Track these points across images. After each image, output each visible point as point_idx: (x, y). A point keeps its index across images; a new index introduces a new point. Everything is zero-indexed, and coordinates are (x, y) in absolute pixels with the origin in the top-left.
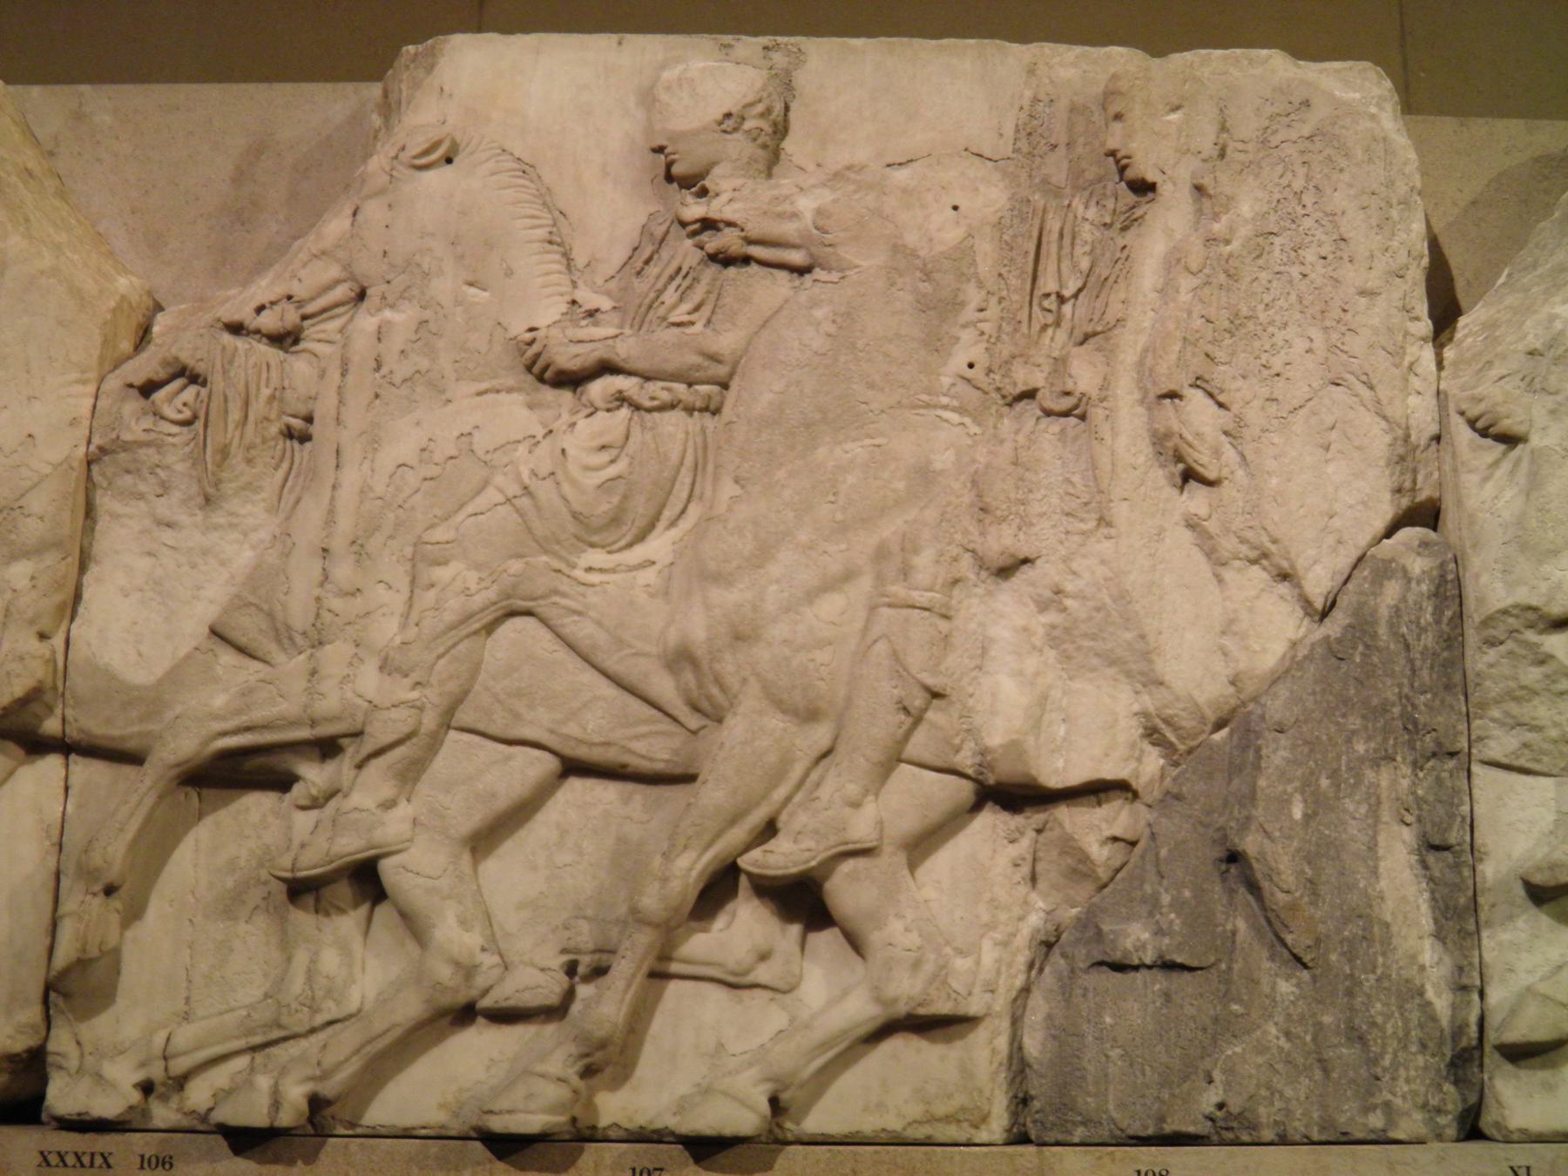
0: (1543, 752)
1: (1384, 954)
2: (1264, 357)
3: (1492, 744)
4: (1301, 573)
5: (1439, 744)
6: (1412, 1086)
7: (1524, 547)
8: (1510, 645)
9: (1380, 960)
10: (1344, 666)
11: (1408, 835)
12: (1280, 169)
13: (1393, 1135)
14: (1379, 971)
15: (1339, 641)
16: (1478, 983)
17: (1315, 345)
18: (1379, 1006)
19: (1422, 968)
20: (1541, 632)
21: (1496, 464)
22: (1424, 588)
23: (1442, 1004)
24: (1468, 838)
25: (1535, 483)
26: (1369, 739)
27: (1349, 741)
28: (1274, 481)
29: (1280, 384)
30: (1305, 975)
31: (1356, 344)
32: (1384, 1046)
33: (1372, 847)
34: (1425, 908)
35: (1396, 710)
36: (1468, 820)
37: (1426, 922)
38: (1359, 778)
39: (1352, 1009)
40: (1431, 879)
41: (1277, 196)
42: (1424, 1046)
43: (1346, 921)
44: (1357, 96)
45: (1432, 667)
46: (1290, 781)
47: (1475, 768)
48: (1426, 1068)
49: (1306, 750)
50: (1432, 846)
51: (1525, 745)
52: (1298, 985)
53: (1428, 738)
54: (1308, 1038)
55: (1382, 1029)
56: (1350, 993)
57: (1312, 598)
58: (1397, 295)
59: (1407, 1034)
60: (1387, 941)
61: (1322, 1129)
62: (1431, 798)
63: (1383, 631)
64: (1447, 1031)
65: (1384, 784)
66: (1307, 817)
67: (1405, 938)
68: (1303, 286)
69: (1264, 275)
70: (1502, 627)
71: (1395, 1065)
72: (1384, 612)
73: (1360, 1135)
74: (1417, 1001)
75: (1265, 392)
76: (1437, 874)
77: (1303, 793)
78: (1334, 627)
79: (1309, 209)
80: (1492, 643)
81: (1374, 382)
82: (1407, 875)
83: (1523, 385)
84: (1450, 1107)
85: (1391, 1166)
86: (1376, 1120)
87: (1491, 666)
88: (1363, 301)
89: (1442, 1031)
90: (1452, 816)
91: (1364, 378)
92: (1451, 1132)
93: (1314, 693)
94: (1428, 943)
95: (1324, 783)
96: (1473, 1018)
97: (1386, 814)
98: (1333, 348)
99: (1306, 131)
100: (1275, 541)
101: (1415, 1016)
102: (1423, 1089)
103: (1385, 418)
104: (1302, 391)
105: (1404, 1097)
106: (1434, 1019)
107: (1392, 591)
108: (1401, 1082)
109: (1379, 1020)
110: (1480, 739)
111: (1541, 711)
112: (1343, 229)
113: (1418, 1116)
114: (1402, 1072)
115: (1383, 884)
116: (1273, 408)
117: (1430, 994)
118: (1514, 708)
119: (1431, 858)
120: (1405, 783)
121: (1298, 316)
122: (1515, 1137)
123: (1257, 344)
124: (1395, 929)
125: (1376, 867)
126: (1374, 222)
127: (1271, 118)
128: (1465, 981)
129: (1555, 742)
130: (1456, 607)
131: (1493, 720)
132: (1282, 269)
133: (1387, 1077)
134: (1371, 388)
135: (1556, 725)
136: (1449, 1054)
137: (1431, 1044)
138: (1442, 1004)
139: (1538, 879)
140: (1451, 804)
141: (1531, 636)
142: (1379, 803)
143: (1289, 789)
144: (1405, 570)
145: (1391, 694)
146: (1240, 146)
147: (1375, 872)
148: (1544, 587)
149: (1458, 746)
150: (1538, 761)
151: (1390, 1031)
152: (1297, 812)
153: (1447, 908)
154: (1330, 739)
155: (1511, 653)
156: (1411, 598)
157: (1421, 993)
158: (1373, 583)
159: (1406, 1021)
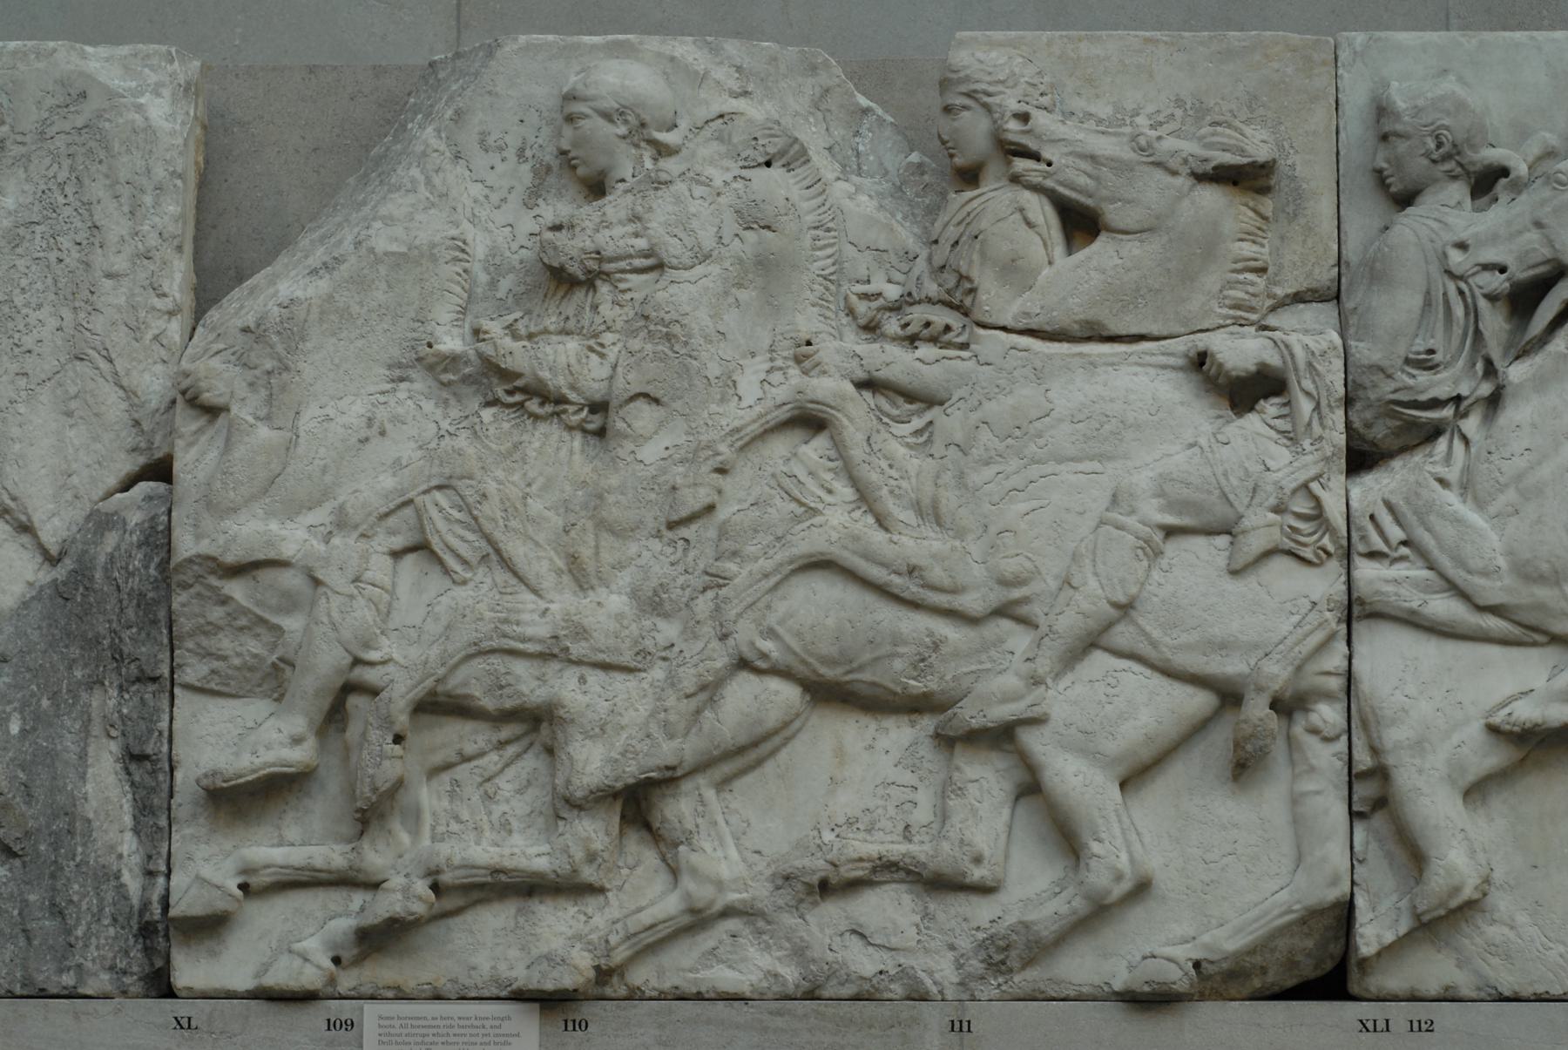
0: (228, 677)
1: (84, 845)
2: (17, 336)
3: (188, 670)
4: (36, 525)
5: (142, 671)
6: (102, 949)
7: (209, 505)
8: (198, 588)
9: (80, 849)
10: (69, 604)
11: (114, 747)
12: (47, 161)
13: (81, 991)
14: (78, 859)
15: (64, 584)
16: (163, 868)
17: (65, 324)
18: (76, 887)
19: (120, 856)
20: (220, 578)
21: (200, 431)
22: (135, 538)
23: (133, 883)
24: (165, 749)
25: (228, 445)
26: (86, 666)
27: (70, 668)
28: (17, 446)
29: (29, 359)
30: (17, 862)
31: (98, 323)
32: (78, 919)
33: (83, 756)
34: (127, 807)
35: (106, 642)
36: (166, 734)
37: (128, 820)
38: (76, 697)
39: (54, 889)
40: (133, 784)
41: (44, 187)
42: (115, 920)
43: (55, 817)
44: (134, 84)
45: (138, 605)
46: (10, 702)
47: (177, 691)
48: (116, 938)
49: (28, 676)
50: (134, 758)
51: (213, 672)
52: (10, 870)
53: (132, 666)
54: (16, 912)
55: (77, 905)
56: (53, 876)
57: (48, 546)
58: (142, 275)
59: (101, 910)
60: (88, 835)
61: (24, 985)
62: (135, 716)
63: (98, 575)
64: (136, 907)
65: (95, 704)
66: (23, 732)
67: (106, 832)
68: (59, 270)
69: (21, 263)
70: (190, 573)
71: (88, 935)
72: (102, 559)
73: (55, 991)
74: (113, 883)
75: (15, 367)
76: (137, 778)
77: (21, 713)
78: (60, 573)
79: (71, 198)
80: (185, 586)
81: (113, 356)
82: (112, 779)
83: (233, 358)
84: (135, 969)
85: (76, 1016)
86: (68, 979)
87: (183, 605)
88: (108, 283)
89: (132, 907)
90: (150, 731)
91: (104, 353)
92: (136, 988)
93: (39, 628)
94: (129, 836)
95: (45, 703)
96: (155, 898)
97: (96, 729)
98: (78, 326)
99: (79, 123)
100: (14, 499)
101: (109, 897)
102: (111, 955)
103: (122, 387)
104: (50, 364)
105: (93, 960)
106: (126, 898)
107: (111, 540)
108: (93, 948)
109: (75, 898)
110: (180, 666)
111: (225, 643)
112: (96, 217)
113: (105, 977)
114: (93, 940)
115: (89, 787)
116: (22, 382)
117: (126, 877)
118: (205, 642)
119: (133, 767)
120: (112, 703)
121: (52, 297)
122: (184, 994)
123: (10, 325)
124: (96, 824)
125: (85, 773)
126: (126, 209)
127: (50, 110)
128: (151, 867)
129: (238, 669)
130: (163, 554)
131: (189, 650)
132: (41, 254)
133: (81, 943)
134: (111, 361)
135: (238, 655)
136: (136, 927)
137: (120, 919)
138: (133, 883)
139: (205, 782)
140: (151, 719)
141: (213, 581)
142: (90, 720)
143: (8, 709)
144: (125, 523)
145: (102, 629)
146: (19, 138)
147: (83, 777)
148: (221, 540)
149: (157, 673)
150: (228, 685)
151: (84, 907)
152: (15, 728)
153: (145, 807)
154: (52, 666)
155: (199, 594)
156: (123, 547)
157: (118, 876)
158: (95, 534)
159: (101, 900)
